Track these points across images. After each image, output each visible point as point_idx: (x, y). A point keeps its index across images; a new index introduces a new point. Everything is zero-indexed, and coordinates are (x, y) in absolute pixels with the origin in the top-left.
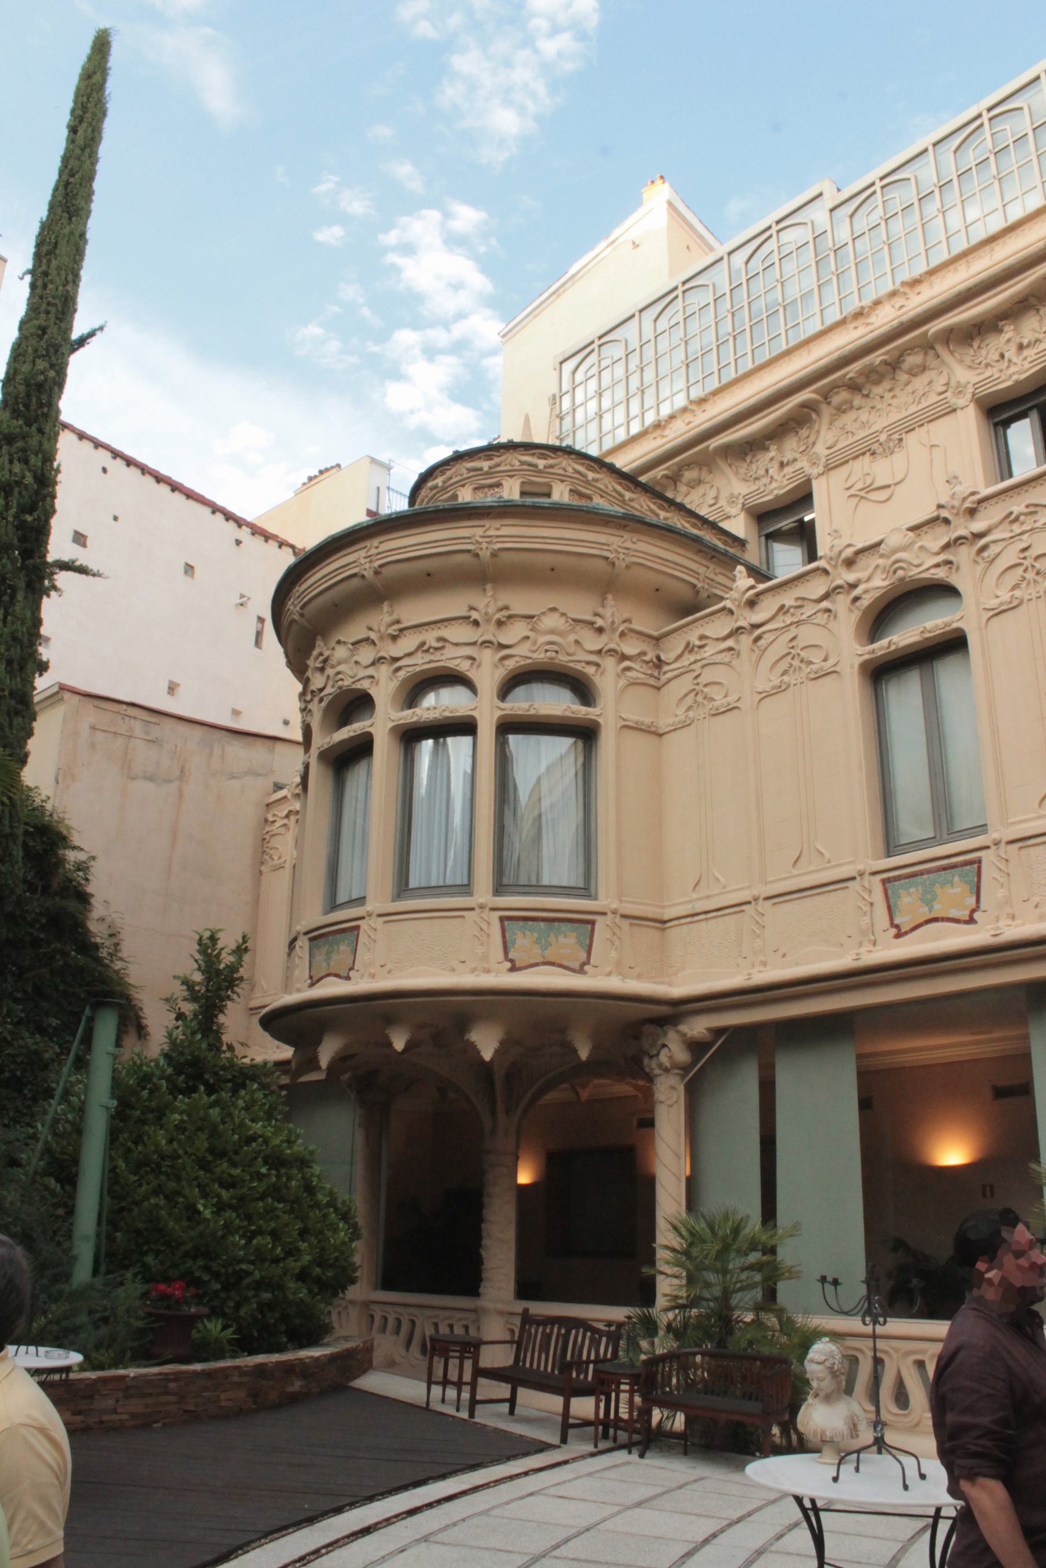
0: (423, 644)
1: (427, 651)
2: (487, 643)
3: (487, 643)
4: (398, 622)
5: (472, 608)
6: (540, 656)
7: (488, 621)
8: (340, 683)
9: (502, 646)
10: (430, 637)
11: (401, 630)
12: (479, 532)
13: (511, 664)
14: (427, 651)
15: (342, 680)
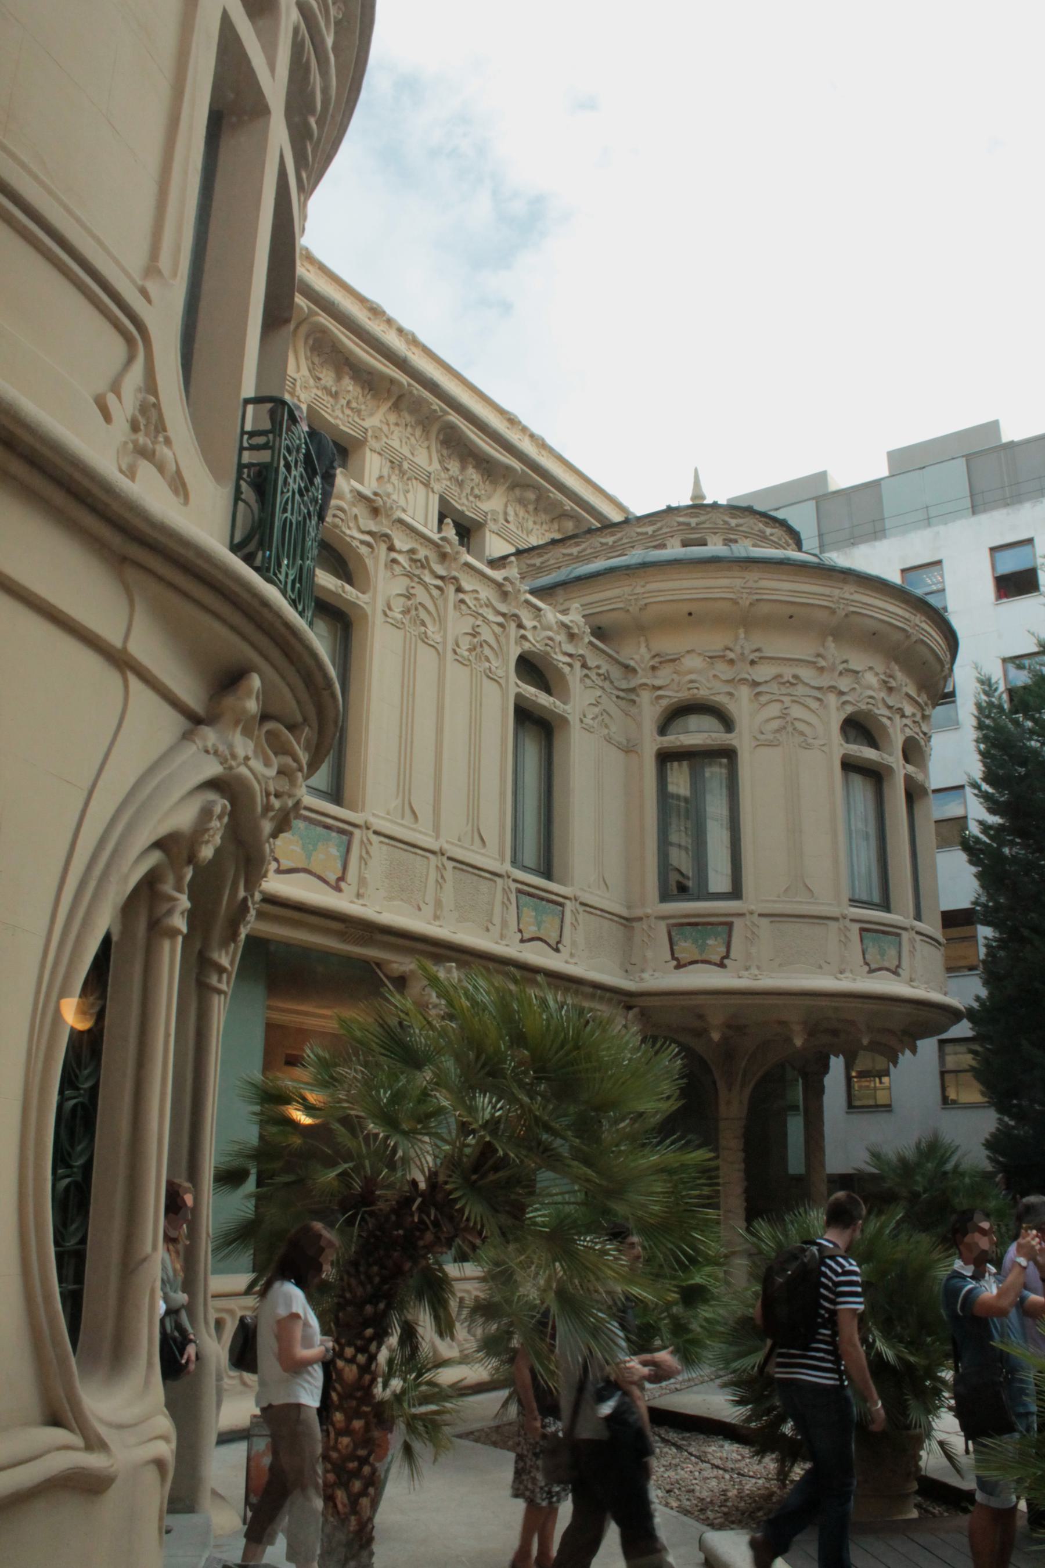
0: (780, 676)
1: (784, 683)
2: (832, 688)
3: (832, 688)
4: (758, 650)
5: (819, 655)
6: (864, 707)
7: (833, 669)
8: (695, 691)
9: (842, 693)
10: (788, 672)
11: (760, 658)
12: (836, 592)
13: (849, 709)
14: (784, 683)
15: (697, 688)
